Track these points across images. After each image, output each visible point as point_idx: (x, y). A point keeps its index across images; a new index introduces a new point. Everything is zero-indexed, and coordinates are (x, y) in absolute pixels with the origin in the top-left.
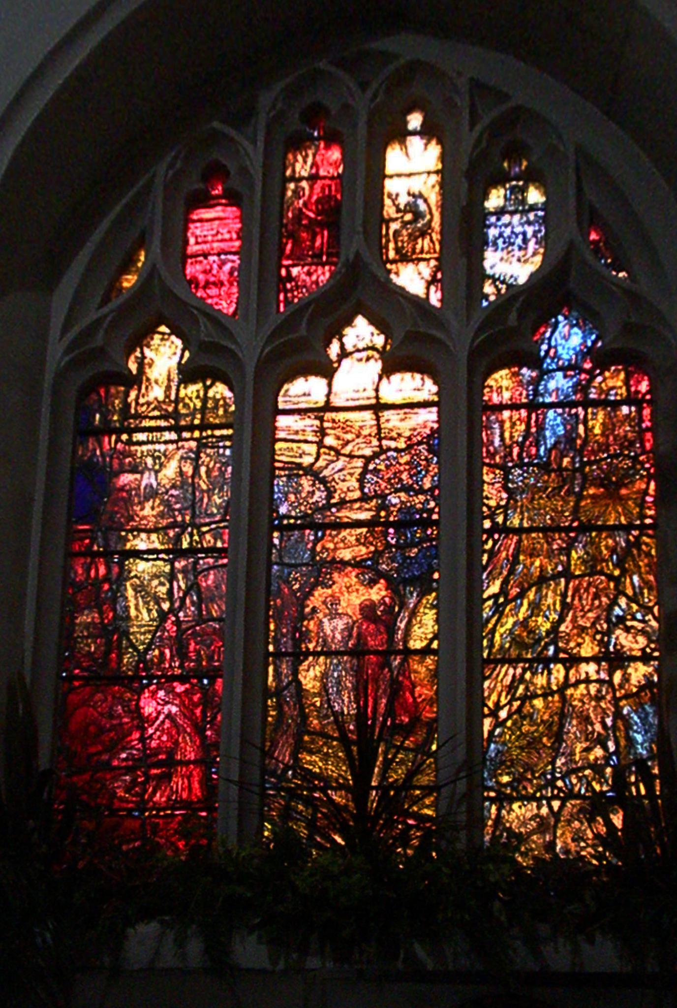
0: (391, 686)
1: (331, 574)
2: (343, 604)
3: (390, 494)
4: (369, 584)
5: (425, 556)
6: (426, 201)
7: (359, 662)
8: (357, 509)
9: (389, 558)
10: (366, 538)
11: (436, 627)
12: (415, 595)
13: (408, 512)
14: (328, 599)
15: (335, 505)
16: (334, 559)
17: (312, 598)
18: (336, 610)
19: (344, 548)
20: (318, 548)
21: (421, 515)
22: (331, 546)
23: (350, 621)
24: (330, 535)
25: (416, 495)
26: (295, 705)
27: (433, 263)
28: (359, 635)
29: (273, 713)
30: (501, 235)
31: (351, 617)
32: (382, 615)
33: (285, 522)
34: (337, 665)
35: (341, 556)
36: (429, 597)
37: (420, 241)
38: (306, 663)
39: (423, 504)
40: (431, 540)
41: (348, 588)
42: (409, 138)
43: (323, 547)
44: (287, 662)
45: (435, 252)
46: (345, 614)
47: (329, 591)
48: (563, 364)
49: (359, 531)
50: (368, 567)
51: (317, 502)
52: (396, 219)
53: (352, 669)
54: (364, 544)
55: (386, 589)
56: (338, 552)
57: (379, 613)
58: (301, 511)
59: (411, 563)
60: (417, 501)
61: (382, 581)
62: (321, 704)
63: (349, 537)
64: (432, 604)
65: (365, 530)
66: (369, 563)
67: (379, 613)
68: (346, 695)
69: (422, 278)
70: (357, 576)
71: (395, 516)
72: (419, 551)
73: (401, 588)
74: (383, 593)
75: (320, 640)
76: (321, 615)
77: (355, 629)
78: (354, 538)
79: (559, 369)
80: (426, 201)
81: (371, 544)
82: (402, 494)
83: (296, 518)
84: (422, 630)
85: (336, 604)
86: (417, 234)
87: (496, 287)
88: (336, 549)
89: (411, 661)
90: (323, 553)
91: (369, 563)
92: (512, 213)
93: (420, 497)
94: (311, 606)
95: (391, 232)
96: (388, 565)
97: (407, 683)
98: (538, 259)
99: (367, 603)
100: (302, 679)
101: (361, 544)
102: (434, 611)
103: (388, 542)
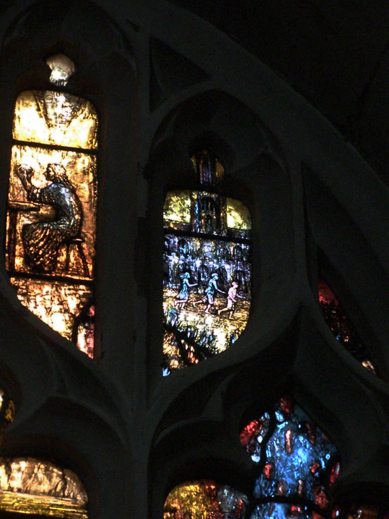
6: (73, 191)
27: (83, 289)
30: (186, 268)
37: (64, 251)
42: (49, 94)
45: (86, 275)
48: (285, 491)
52: (28, 210)
69: (67, 311)
79: (280, 499)
80: (73, 191)
86: (60, 240)
87: (180, 346)
92: (204, 238)
95: (19, 226)
98: (242, 315)
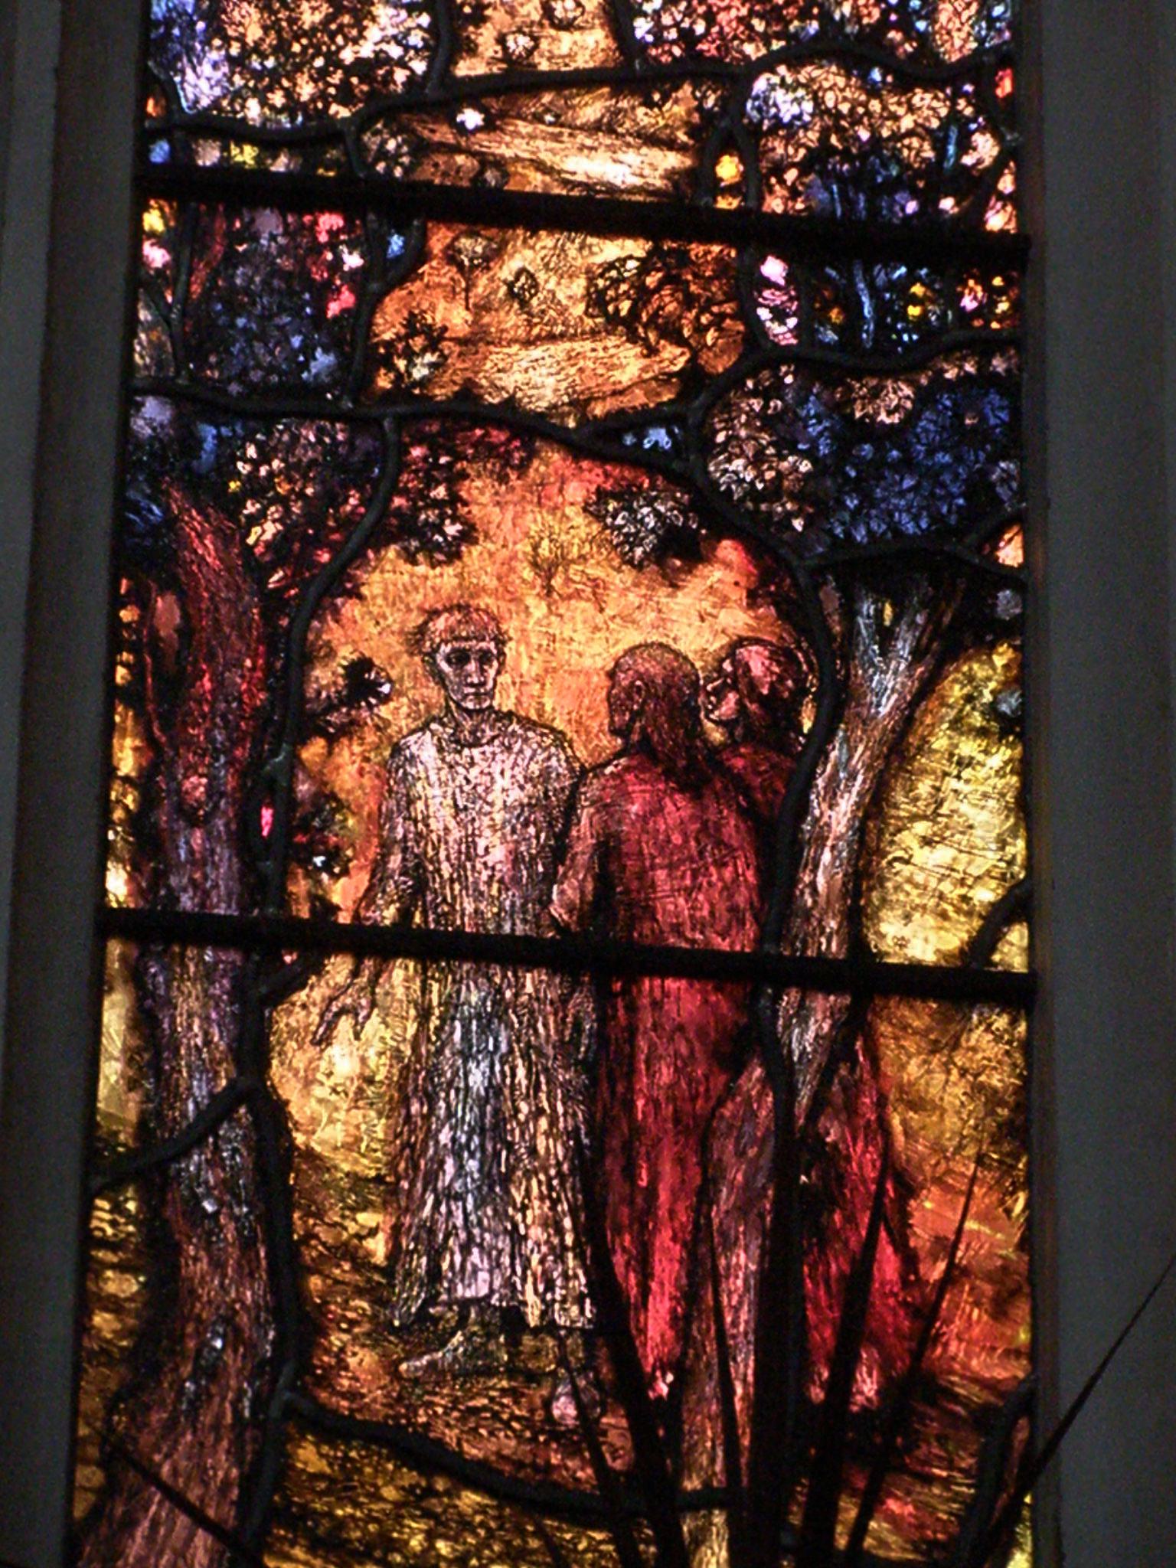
0: (783, 1169)
1: (455, 479)
2: (521, 658)
3: (768, 64)
4: (659, 555)
5: (957, 437)
7: (604, 1019)
8: (594, 128)
9: (768, 422)
10: (642, 295)
11: (1018, 847)
12: (903, 648)
13: (860, 179)
14: (440, 623)
15: (475, 92)
16: (468, 392)
17: (351, 609)
18: (482, 692)
19: (528, 343)
20: (388, 325)
21: (929, 202)
22: (456, 318)
23: (559, 765)
24: (451, 256)
25: (904, 85)
26: (247, 1245)
28: (608, 849)
29: (122, 1285)
31: (560, 739)
32: (732, 745)
33: (209, 155)
34: (487, 1022)
35: (509, 381)
36: (979, 670)
38: (315, 993)
39: (938, 140)
40: (985, 346)
41: (546, 570)
43: (414, 324)
44: (208, 974)
46: (528, 723)
47: (446, 578)
49: (610, 250)
50: (651, 462)
51: (381, 59)
53: (566, 1048)
54: (629, 327)
55: (753, 599)
56: (497, 357)
57: (717, 736)
58: (293, 105)
59: (879, 464)
60: (907, 123)
61: (728, 549)
62: (395, 1253)
63: (548, 282)
64: (992, 711)
65: (636, 248)
66: (659, 436)
67: (717, 736)
68: (538, 1208)
70: (595, 509)
71: (794, 193)
72: (924, 398)
73: (830, 598)
74: (737, 619)
75: (395, 862)
76: (396, 714)
77: (585, 814)
78: (579, 286)
81: (671, 333)
82: (830, 78)
83: (268, 140)
84: (943, 855)
85: (484, 658)
88: (476, 340)
89: (884, 1028)
90: (410, 355)
91: (659, 436)
93: (921, 98)
94: (346, 654)
96: (757, 460)
97: (864, 1161)
99: (653, 669)
100: (289, 1090)
101: (613, 322)
102: (1002, 755)
103: (756, 328)
